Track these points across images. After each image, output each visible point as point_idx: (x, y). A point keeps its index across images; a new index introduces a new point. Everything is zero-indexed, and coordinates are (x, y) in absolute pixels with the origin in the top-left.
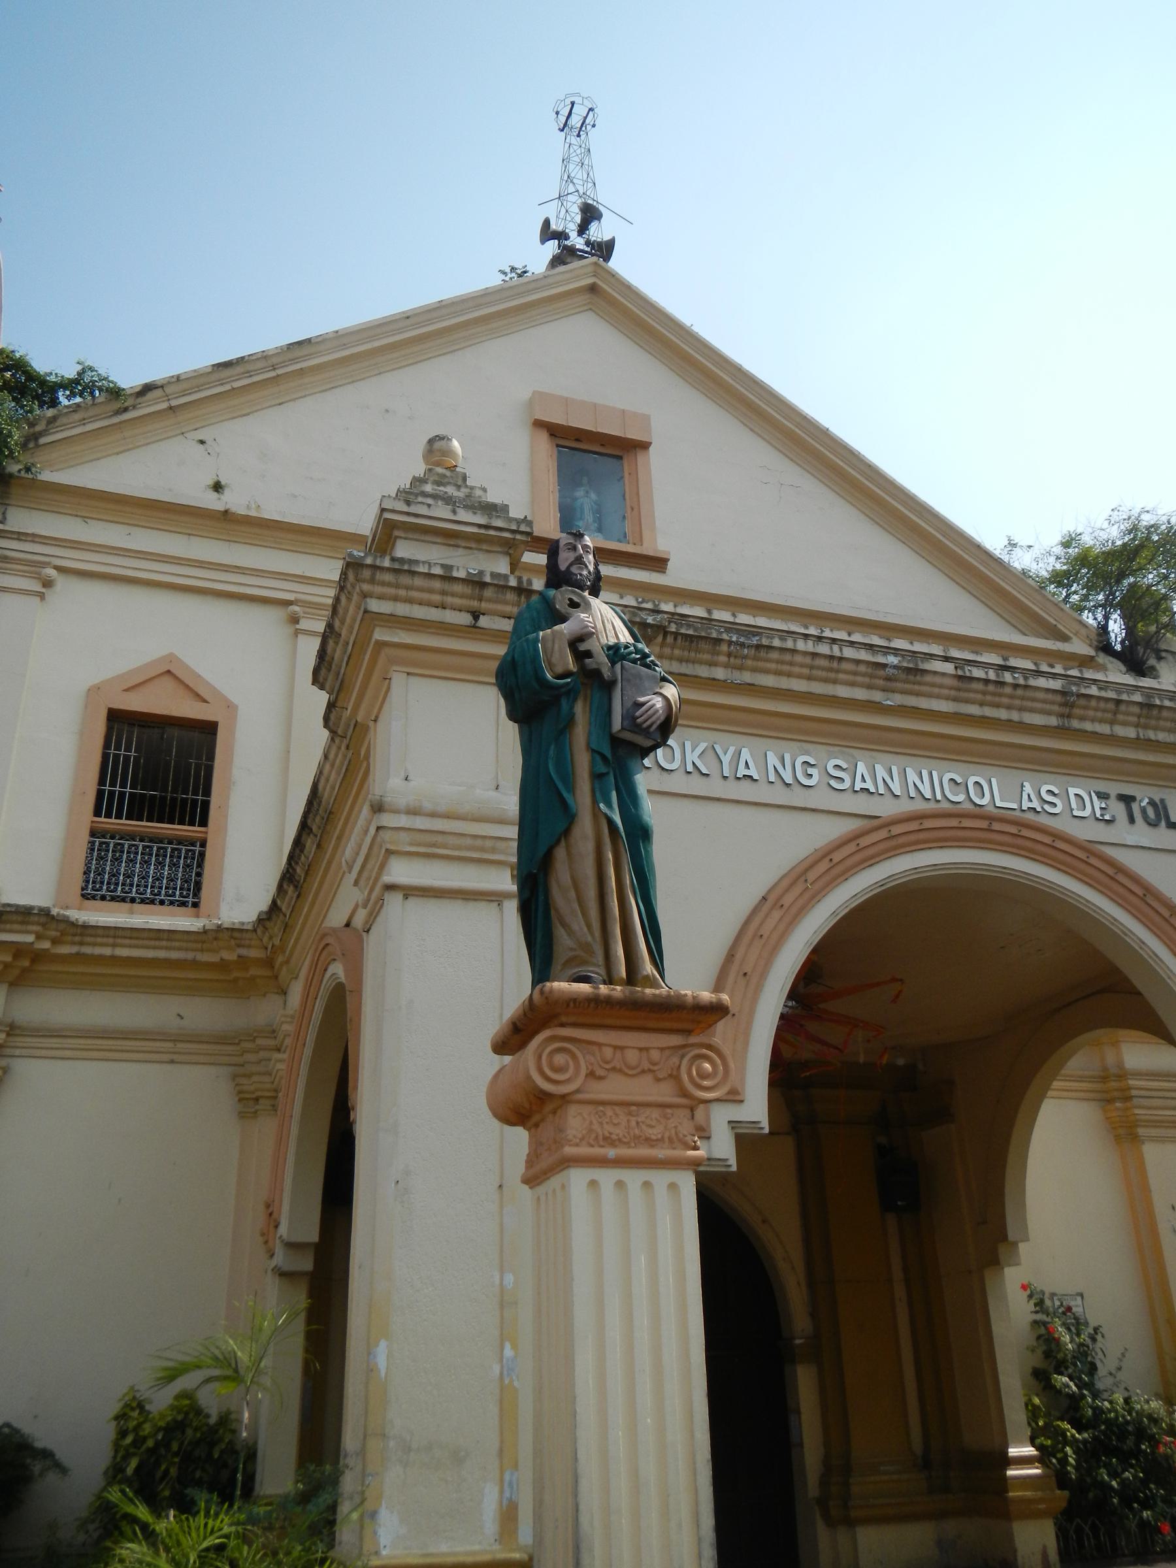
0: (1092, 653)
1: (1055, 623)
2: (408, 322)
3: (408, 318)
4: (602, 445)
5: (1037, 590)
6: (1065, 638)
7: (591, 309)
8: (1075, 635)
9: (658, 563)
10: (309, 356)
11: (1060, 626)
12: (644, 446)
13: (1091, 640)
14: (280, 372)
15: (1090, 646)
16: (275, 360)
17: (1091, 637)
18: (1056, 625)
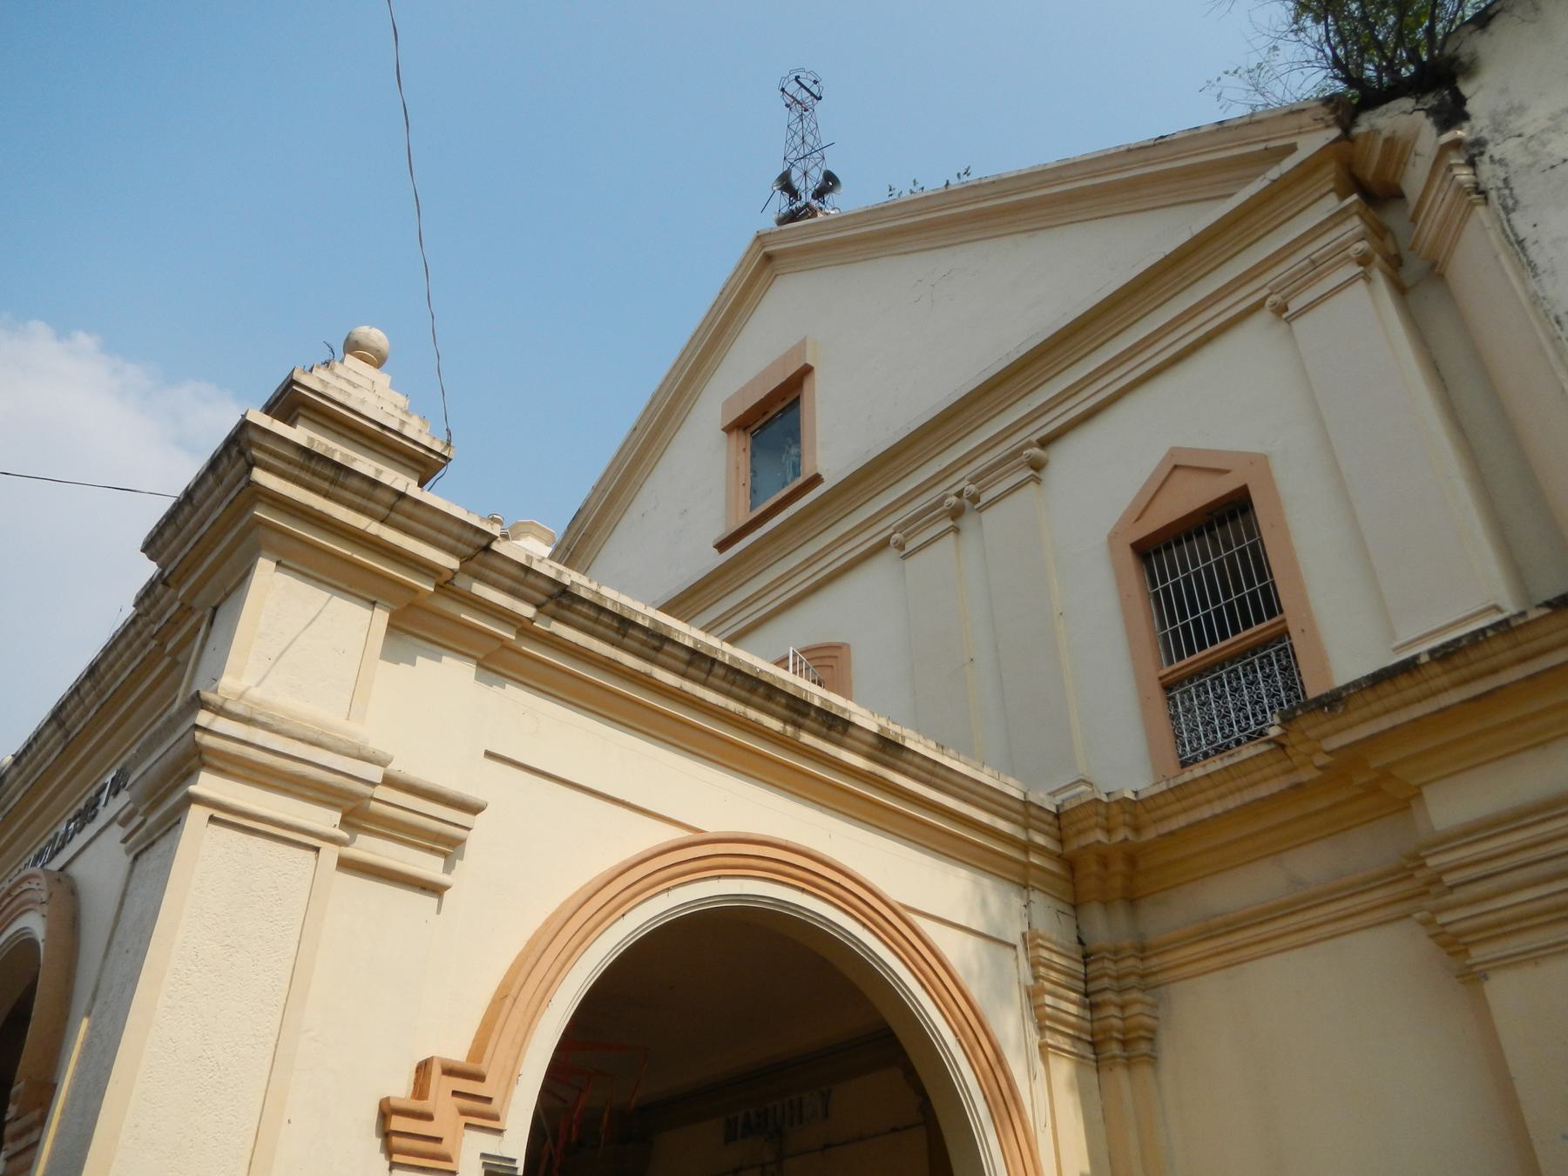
0: (1335, 133)
1: (1261, 146)
2: (638, 432)
3: (635, 429)
4: (782, 400)
5: (1217, 130)
6: (1292, 149)
7: (777, 275)
8: (1300, 133)
9: (816, 480)
10: (586, 519)
11: (1272, 144)
12: (807, 370)
13: (1322, 119)
14: (572, 549)
15: (1328, 127)
16: (565, 544)
17: (1321, 116)
18: (1266, 149)
